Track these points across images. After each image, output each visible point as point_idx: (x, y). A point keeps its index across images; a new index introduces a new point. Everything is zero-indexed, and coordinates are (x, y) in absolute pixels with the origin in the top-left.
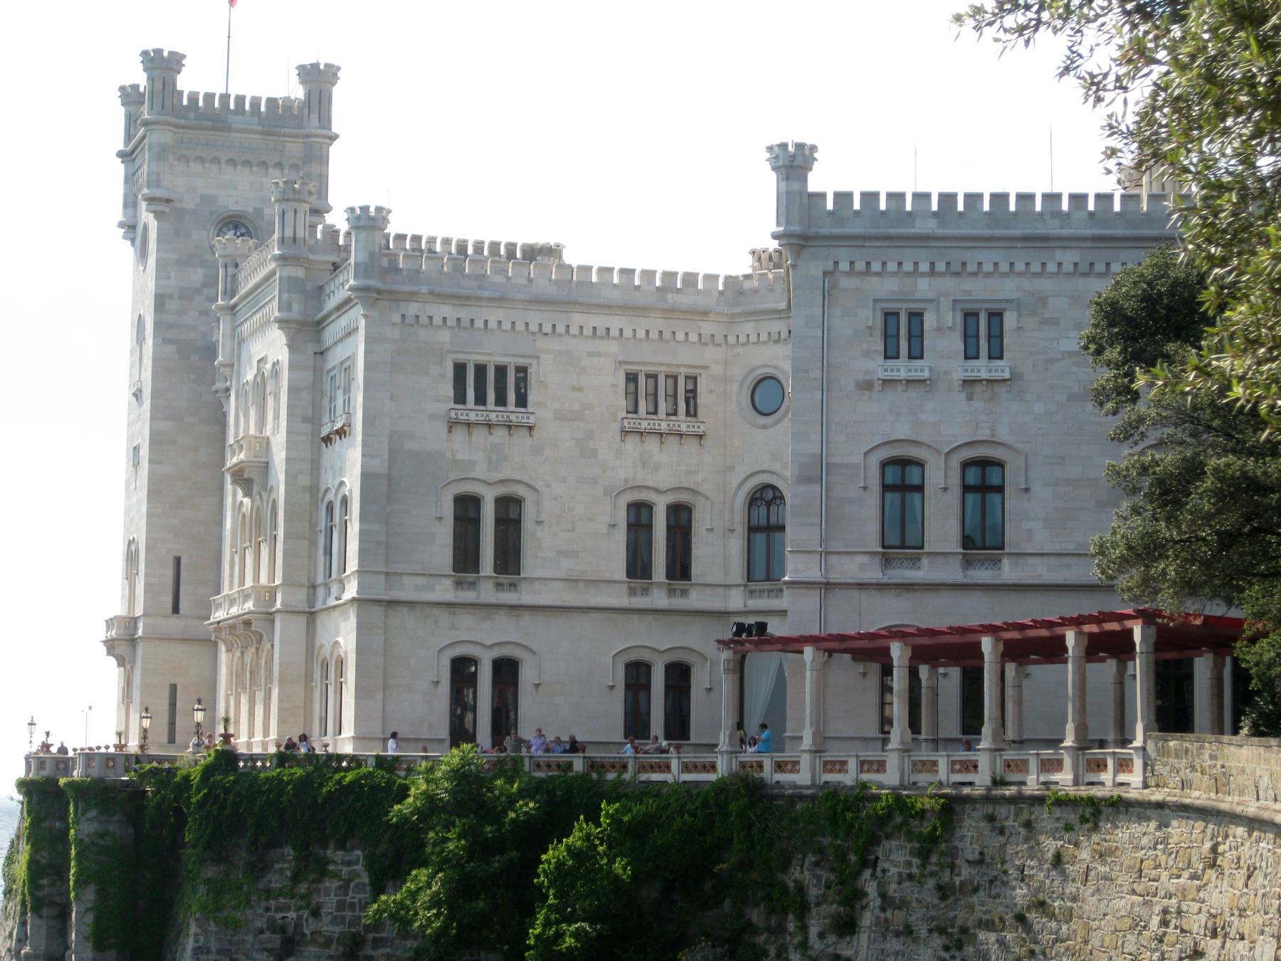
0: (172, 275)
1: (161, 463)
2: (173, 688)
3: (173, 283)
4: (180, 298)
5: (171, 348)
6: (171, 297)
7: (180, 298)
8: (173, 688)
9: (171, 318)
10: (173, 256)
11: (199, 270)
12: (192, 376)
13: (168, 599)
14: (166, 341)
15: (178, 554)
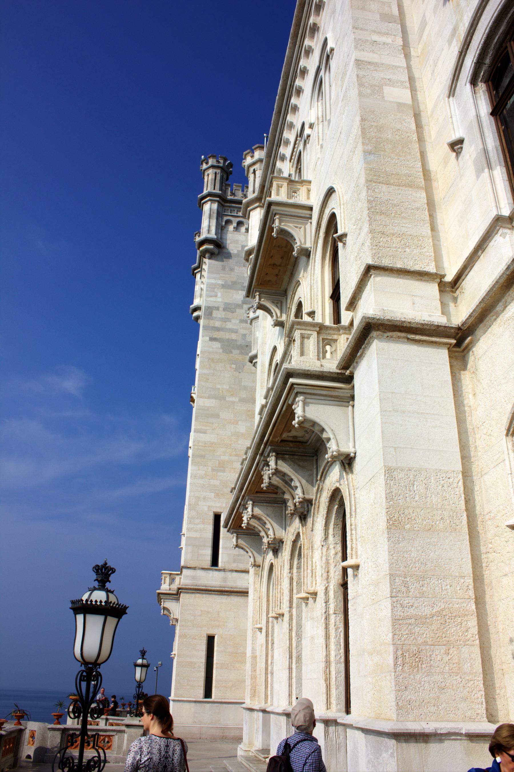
0: (219, 294)
1: (204, 432)
2: (211, 640)
3: (220, 300)
4: (224, 310)
5: (217, 345)
6: (217, 309)
7: (224, 310)
8: (211, 640)
9: (218, 324)
10: (220, 282)
11: (240, 292)
12: (234, 366)
13: (208, 552)
14: (212, 339)
15: (218, 510)
